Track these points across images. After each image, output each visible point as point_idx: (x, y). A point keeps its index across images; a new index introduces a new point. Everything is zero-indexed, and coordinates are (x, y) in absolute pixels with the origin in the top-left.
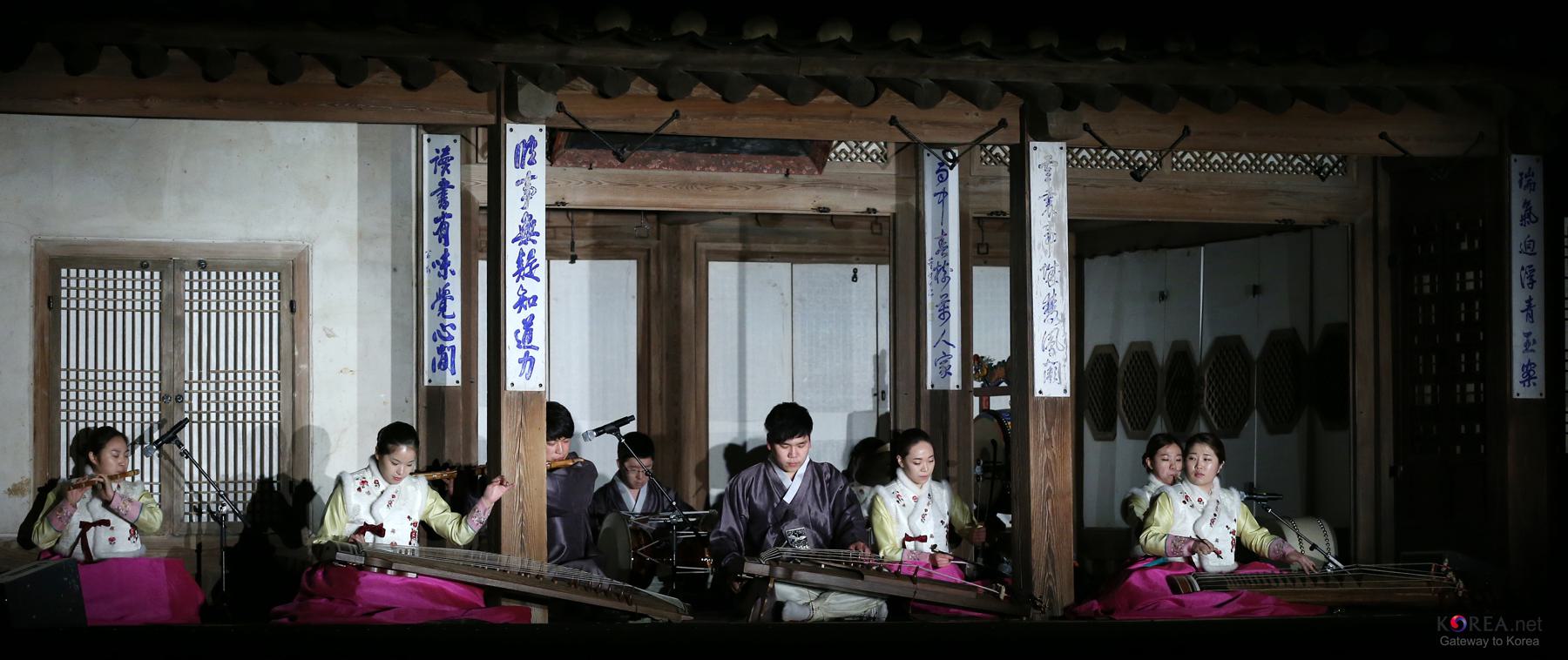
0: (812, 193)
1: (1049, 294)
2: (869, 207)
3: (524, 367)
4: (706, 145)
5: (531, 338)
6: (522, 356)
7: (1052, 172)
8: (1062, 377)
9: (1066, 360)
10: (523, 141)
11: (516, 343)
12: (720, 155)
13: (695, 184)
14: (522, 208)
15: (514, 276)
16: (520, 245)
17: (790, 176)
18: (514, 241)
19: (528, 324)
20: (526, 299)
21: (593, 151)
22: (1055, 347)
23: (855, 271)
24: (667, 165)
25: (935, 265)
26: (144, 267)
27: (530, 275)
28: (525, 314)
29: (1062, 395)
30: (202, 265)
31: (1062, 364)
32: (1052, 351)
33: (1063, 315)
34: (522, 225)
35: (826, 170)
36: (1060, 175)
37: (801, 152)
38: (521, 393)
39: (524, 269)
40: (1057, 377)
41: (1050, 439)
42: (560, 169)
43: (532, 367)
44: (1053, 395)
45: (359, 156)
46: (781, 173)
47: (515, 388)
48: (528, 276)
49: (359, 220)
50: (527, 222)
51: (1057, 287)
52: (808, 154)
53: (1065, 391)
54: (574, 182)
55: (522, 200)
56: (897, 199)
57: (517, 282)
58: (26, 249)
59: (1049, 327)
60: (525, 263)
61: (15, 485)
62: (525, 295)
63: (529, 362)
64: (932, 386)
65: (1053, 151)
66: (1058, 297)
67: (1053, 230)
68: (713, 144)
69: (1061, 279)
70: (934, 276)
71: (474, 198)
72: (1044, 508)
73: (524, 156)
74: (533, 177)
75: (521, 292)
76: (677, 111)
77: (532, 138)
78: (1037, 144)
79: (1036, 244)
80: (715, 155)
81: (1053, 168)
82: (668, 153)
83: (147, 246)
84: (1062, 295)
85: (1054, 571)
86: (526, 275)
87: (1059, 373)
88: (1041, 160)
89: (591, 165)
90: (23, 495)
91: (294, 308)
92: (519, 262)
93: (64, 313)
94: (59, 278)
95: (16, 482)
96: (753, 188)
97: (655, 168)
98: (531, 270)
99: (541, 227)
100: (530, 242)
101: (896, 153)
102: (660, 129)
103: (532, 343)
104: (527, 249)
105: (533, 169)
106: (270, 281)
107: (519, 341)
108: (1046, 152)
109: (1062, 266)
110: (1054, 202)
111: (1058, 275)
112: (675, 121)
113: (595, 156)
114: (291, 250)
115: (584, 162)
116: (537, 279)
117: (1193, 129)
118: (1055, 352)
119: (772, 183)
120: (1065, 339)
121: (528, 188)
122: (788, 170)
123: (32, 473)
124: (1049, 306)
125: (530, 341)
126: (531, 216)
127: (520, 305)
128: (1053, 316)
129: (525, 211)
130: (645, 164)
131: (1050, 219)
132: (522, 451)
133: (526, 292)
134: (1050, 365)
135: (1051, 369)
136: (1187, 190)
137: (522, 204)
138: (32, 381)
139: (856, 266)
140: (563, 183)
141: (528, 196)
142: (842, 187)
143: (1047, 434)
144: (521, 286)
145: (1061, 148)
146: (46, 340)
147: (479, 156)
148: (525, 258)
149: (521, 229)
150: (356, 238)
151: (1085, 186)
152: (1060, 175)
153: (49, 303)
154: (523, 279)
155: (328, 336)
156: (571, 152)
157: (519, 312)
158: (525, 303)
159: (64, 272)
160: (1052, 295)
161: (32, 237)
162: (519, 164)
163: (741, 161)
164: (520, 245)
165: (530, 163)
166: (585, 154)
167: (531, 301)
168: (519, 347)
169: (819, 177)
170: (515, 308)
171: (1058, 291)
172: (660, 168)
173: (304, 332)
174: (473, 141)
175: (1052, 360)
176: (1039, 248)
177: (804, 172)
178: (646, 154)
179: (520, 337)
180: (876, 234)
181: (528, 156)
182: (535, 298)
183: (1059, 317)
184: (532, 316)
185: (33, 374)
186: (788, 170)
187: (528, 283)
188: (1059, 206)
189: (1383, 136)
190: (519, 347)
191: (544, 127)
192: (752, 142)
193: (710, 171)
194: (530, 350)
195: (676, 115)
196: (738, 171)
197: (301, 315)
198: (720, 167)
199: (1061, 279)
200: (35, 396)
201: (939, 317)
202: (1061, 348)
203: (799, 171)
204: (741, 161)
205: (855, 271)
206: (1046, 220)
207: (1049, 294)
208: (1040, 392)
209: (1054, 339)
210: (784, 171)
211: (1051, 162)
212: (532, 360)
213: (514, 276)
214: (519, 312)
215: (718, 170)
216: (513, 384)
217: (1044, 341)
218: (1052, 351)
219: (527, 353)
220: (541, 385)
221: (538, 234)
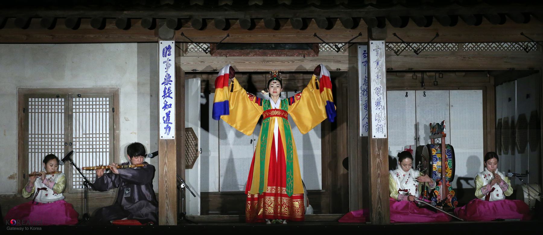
1: (378, 99)
2: (337, 68)
3: (166, 130)
4: (270, 47)
5: (169, 120)
6: (166, 126)
7: (379, 52)
8: (384, 130)
9: (385, 124)
10: (166, 47)
11: (164, 122)
12: (277, 50)
13: (268, 61)
14: (166, 72)
15: (162, 97)
16: (165, 85)
17: (306, 57)
18: (162, 84)
19: (168, 115)
20: (167, 105)
21: (227, 50)
22: (380, 119)
23: (407, 93)
24: (256, 55)
25: (363, 89)
26: (58, 97)
27: (169, 96)
28: (167, 111)
29: (384, 137)
30: (79, 96)
31: (384, 126)
32: (379, 121)
33: (384, 107)
34: (166, 78)
35: (319, 54)
36: (383, 53)
37: (309, 48)
38: (165, 140)
39: (166, 94)
40: (381, 131)
41: (379, 154)
42: (215, 57)
43: (169, 130)
44: (380, 137)
45: (138, 55)
46: (301, 56)
47: (163, 138)
48: (168, 97)
49: (138, 78)
50: (168, 77)
51: (381, 96)
52: (312, 49)
53: (385, 136)
54: (220, 62)
55: (166, 69)
56: (349, 65)
57: (164, 99)
58: (15, 91)
59: (378, 112)
60: (167, 92)
61: (11, 175)
62: (167, 104)
63: (168, 129)
64: (362, 135)
65: (379, 44)
66: (382, 100)
67: (380, 74)
68: (273, 46)
69: (383, 93)
70: (362, 93)
71: (182, 69)
72: (377, 181)
73: (166, 53)
74: (170, 60)
75: (165, 103)
76: (228, 34)
77: (169, 46)
78: (373, 42)
79: (373, 80)
80: (275, 50)
81: (380, 51)
84: (383, 99)
85: (381, 205)
86: (167, 96)
87: (382, 128)
88: (375, 48)
89: (226, 55)
90: (14, 179)
91: (114, 111)
92: (164, 92)
93: (30, 114)
94: (28, 101)
95: (12, 174)
96: (290, 62)
97: (251, 56)
98: (169, 94)
99: (173, 78)
100: (169, 84)
101: (349, 47)
102: (221, 41)
103: (170, 122)
104: (167, 87)
105: (170, 57)
106: (106, 101)
107: (164, 121)
108: (376, 44)
110: (380, 64)
111: (381, 92)
112: (228, 37)
113: (228, 52)
114: (112, 90)
115: (224, 55)
116: (172, 98)
117: (440, 34)
118: (380, 121)
119: (299, 60)
120: (385, 116)
121: (168, 64)
122: (304, 55)
123: (17, 171)
124: (378, 104)
125: (169, 121)
126: (169, 74)
127: (165, 107)
128: (380, 107)
129: (167, 73)
130: (247, 54)
131: (378, 70)
132: (166, 161)
133: (167, 102)
134: (378, 126)
135: (379, 128)
136: (469, 58)
137: (166, 70)
138: (17, 138)
139: (407, 91)
140: (216, 62)
141: (168, 67)
142: (327, 60)
143: (378, 153)
144: (165, 100)
145: (383, 43)
146: (23, 124)
147: (184, 53)
148: (167, 90)
149: (165, 79)
150: (137, 85)
151: (426, 58)
152: (383, 53)
154: (166, 98)
155: (126, 120)
156: (219, 51)
157: (165, 110)
158: (167, 107)
159: (30, 99)
160: (379, 99)
161: (17, 87)
163: (285, 52)
164: (165, 85)
165: (169, 55)
166: (224, 51)
167: (169, 106)
168: (164, 123)
169: (317, 57)
170: (163, 108)
171: (382, 98)
172: (253, 56)
173: (118, 119)
174: (181, 48)
175: (379, 124)
176: (374, 81)
177: (311, 56)
178: (248, 51)
179: (165, 119)
180: (415, 79)
181: (168, 52)
182: (171, 105)
183: (382, 107)
184: (170, 112)
185: (17, 136)
186: (304, 55)
187: (168, 99)
188: (382, 65)
189: (522, 34)
190: (164, 123)
191: (174, 42)
192: (289, 45)
193: (273, 56)
194: (169, 124)
195: (228, 36)
196: (284, 56)
197: (117, 113)
198: (277, 55)
199: (383, 93)
200: (19, 144)
201: (365, 109)
202: (383, 119)
203: (309, 55)
204: (285, 52)
205: (407, 93)
206: (377, 70)
207: (378, 99)
208: (375, 136)
209: (380, 116)
210: (303, 55)
211: (379, 48)
212: (170, 128)
213: (162, 97)
214: (165, 110)
215: (276, 56)
216: (162, 137)
217: (376, 117)
218: (379, 121)
219: (168, 125)
220: (173, 137)
221: (172, 81)
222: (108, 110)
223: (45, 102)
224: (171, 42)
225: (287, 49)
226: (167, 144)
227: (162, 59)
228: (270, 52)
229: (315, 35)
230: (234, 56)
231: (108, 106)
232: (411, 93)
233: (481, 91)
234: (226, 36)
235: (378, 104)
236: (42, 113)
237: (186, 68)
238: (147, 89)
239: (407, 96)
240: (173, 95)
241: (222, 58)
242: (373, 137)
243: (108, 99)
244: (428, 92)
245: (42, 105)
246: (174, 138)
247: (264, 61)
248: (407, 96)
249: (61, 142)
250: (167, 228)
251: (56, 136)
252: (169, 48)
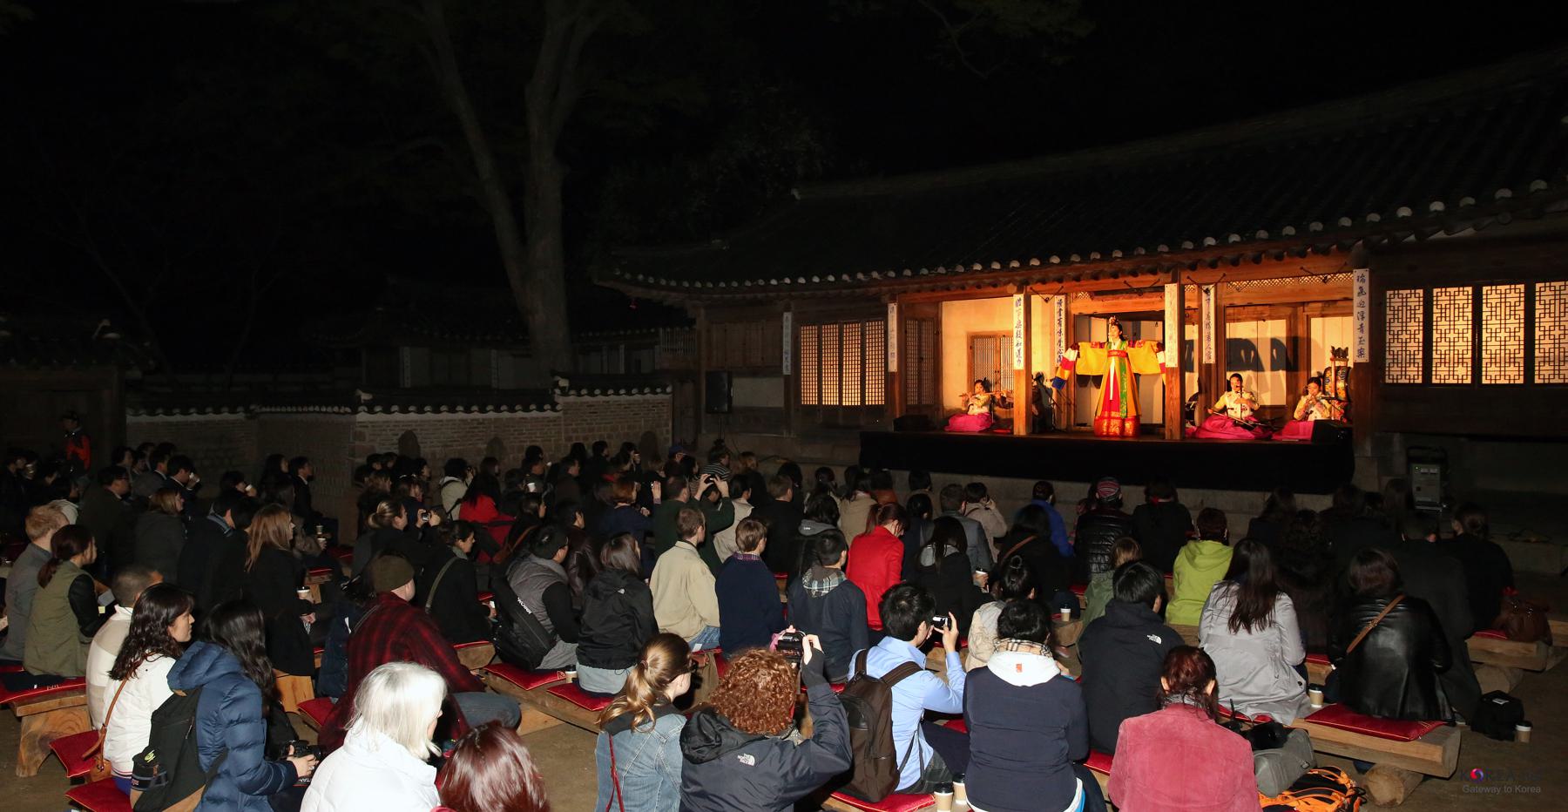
19: (1019, 351)
24: (1124, 298)
28: (1018, 348)
30: (1004, 336)
58: (965, 334)
124: (1171, 338)
130: (1118, 298)
153: (971, 348)
162: (1017, 306)
166: (1101, 297)
178: (1118, 296)
189: (1302, 268)
227: (1015, 308)
233: (1142, 322)
235: (1171, 338)
237: (1075, 312)
238: (1048, 329)
240: (1022, 336)
250: (1020, 439)
252: (1020, 300)
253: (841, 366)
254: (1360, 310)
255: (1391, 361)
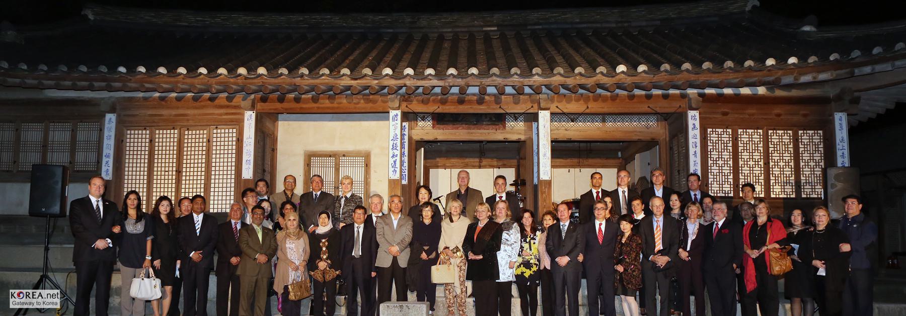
0: (503, 135)
19: (395, 162)
21: (444, 126)
24: (463, 128)
26: (330, 156)
27: (396, 149)
28: (394, 159)
30: (344, 156)
35: (507, 128)
42: (435, 131)
47: (391, 178)
58: (302, 152)
59: (544, 160)
82: (464, 125)
83: (332, 151)
91: (367, 166)
92: (393, 146)
93: (312, 168)
104: (395, 142)
106: (362, 159)
109: (549, 144)
117: (589, 107)
124: (545, 155)
127: (393, 157)
130: (457, 128)
141: (395, 129)
156: (437, 126)
159: (312, 158)
162: (393, 120)
166: (442, 126)
178: (458, 126)
179: (393, 165)
181: (396, 119)
187: (395, 151)
189: (649, 107)
203: (499, 129)
206: (544, 132)
212: (396, 171)
222: (363, 166)
223: (320, 160)
224: (398, 111)
225: (485, 124)
226: (394, 183)
228: (473, 127)
229: (500, 107)
230: (448, 129)
231: (363, 163)
232: (572, 170)
234: (437, 107)
235: (545, 155)
236: (320, 167)
237: (416, 137)
239: (569, 171)
241: (440, 131)
242: (541, 179)
243: (363, 158)
244: (582, 170)
245: (318, 162)
246: (399, 178)
247: (469, 133)
248: (569, 171)
249: (332, 187)
251: (329, 183)
253: (179, 172)
254: (694, 140)
255: (712, 180)
